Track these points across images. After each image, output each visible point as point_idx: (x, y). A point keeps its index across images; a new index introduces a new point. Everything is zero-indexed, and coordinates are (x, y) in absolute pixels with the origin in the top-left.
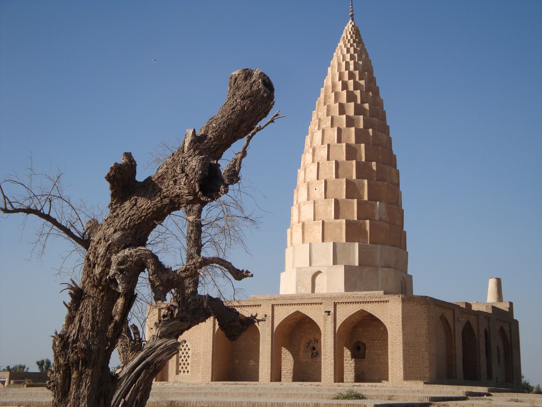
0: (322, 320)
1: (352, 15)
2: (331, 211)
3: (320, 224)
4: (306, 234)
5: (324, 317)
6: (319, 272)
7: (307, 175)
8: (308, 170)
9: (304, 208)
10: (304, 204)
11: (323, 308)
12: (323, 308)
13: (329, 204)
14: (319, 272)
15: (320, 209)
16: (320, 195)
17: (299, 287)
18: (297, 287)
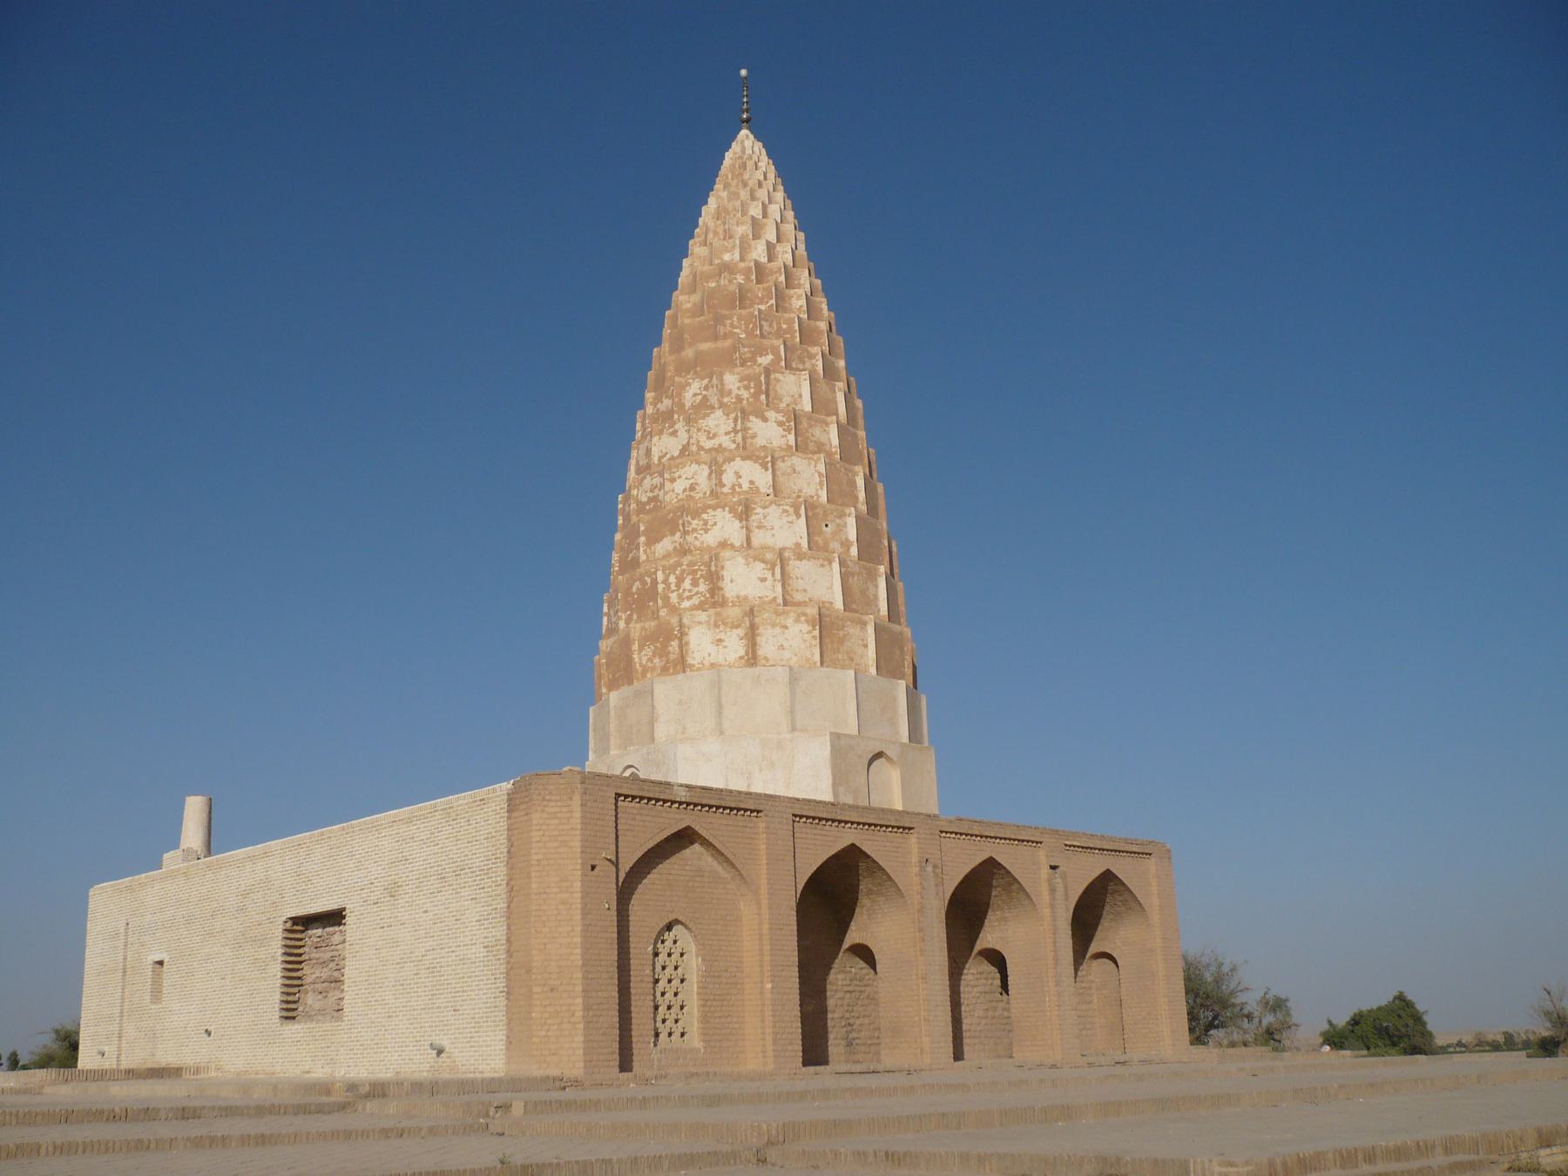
0: (1045, 889)
1: (747, 121)
2: (876, 597)
3: (864, 624)
4: (827, 640)
5: (1050, 881)
6: (879, 755)
7: (781, 479)
8: (780, 464)
9: (799, 568)
10: (800, 556)
11: (1043, 857)
12: (1043, 857)
13: (872, 576)
14: (879, 755)
15: (854, 582)
16: (842, 544)
17: (841, 790)
18: (835, 785)
